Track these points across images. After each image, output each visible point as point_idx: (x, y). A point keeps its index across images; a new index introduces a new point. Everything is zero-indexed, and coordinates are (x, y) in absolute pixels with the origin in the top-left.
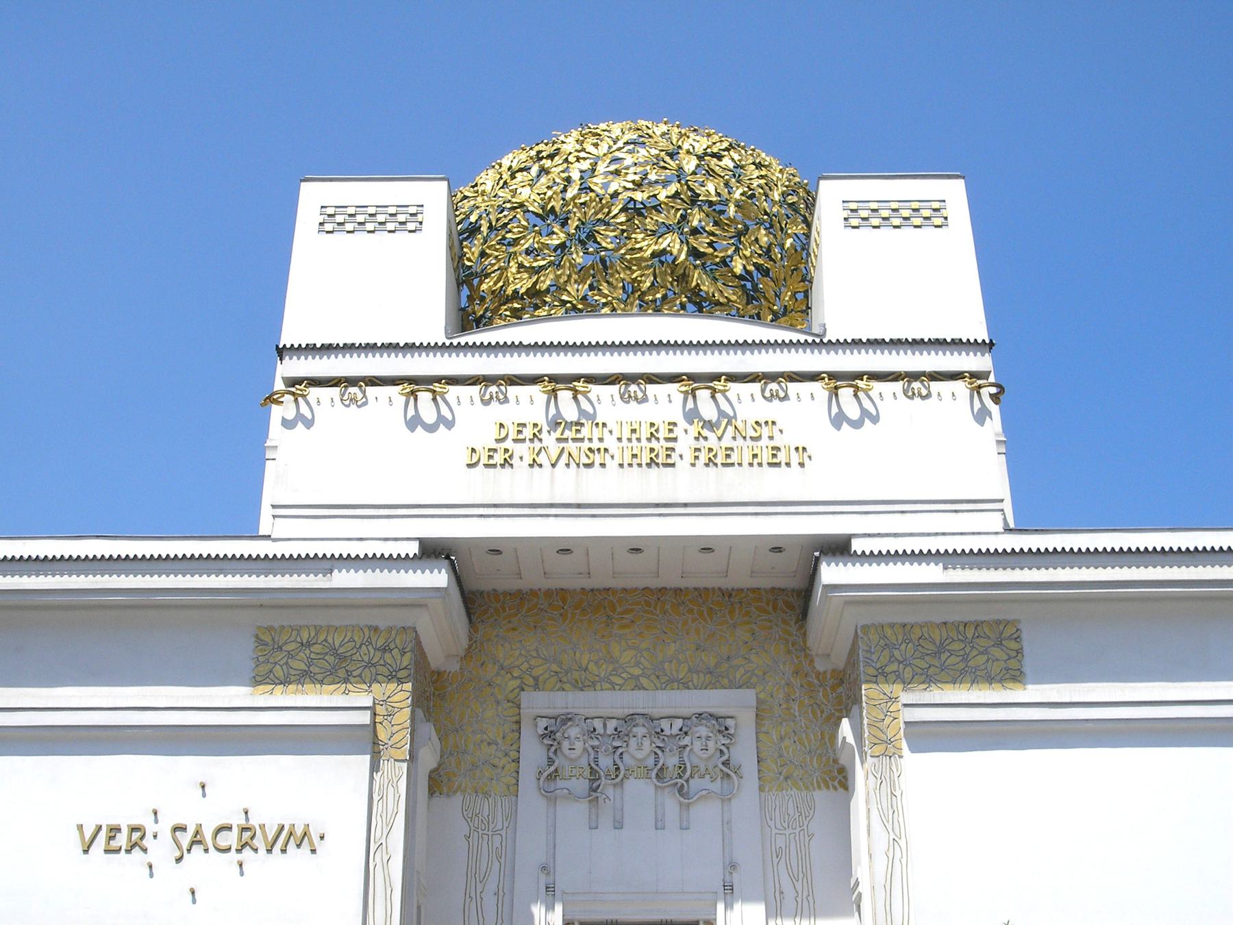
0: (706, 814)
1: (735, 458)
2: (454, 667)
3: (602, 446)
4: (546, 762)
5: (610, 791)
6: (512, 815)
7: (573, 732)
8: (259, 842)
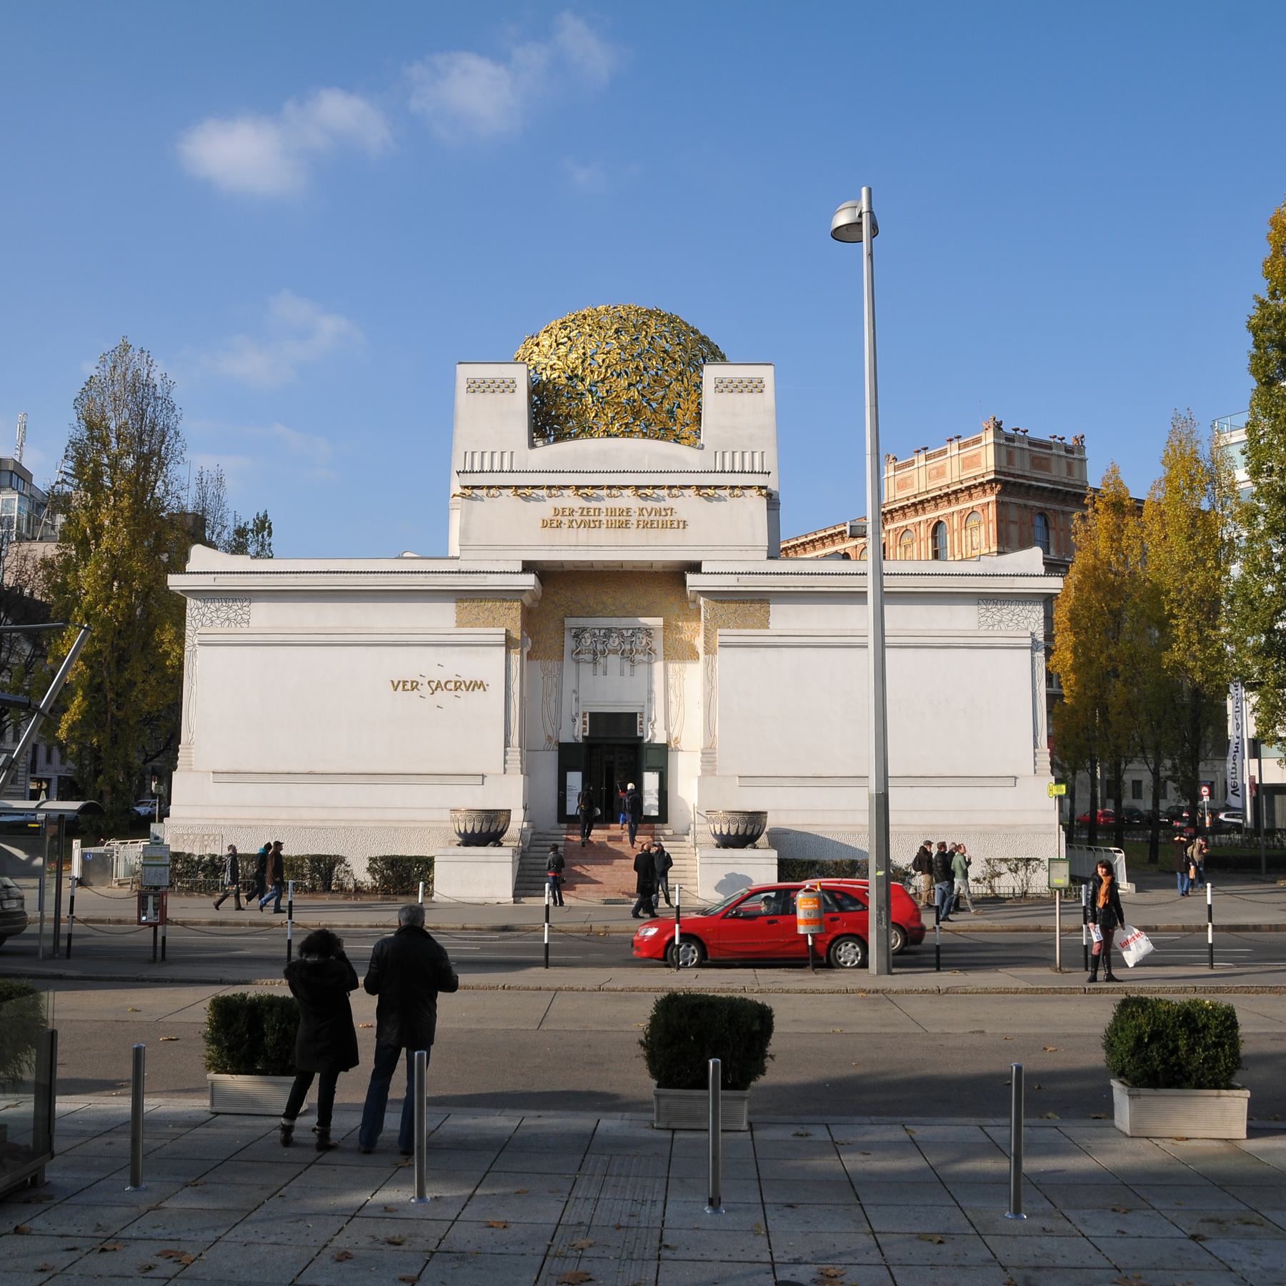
0: (641, 669)
1: (655, 525)
2: (536, 605)
3: (600, 518)
4: (575, 648)
5: (602, 660)
6: (561, 670)
7: (587, 635)
8: (463, 687)
